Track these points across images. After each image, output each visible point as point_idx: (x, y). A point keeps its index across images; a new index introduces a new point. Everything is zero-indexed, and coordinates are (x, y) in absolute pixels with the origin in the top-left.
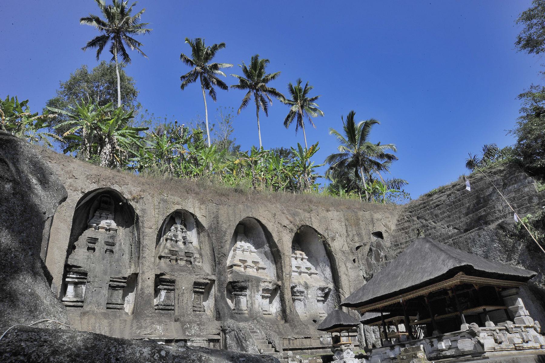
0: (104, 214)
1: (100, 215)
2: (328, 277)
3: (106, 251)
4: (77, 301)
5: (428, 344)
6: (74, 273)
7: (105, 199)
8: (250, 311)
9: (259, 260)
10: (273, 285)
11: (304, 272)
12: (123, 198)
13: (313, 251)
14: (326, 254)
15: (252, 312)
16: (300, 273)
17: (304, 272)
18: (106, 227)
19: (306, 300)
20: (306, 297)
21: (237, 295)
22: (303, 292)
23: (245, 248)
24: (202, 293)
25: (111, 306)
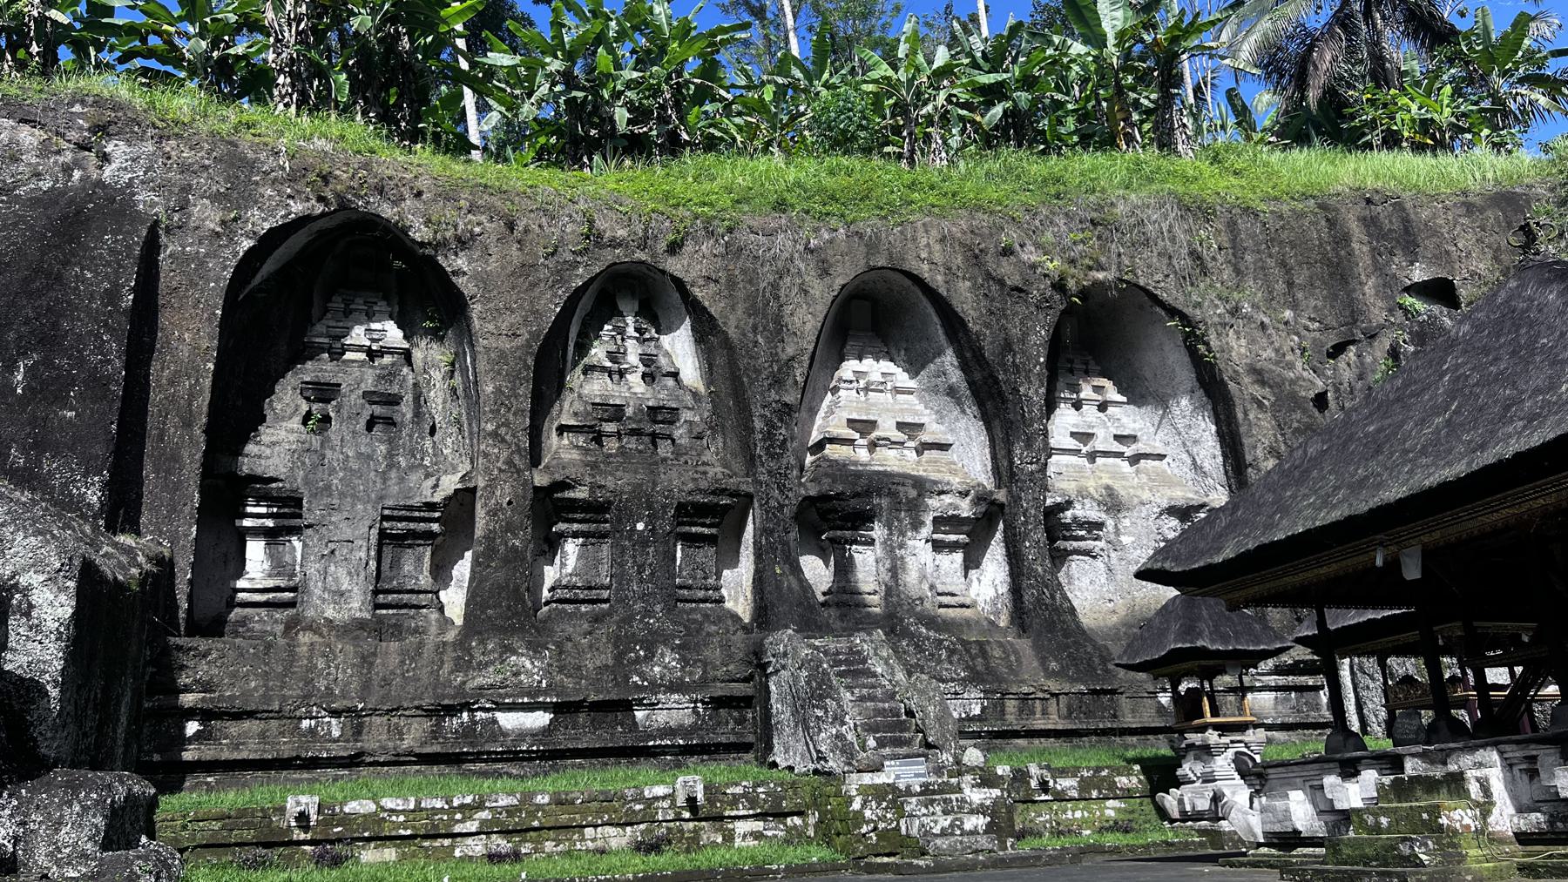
1: (347, 305)
2: (1207, 466)
4: (277, 589)
5: (1516, 769)
8: (889, 592)
9: (926, 417)
11: (1106, 454)
12: (409, 244)
13: (1148, 374)
14: (1198, 380)
15: (895, 599)
16: (1092, 457)
17: (1106, 454)
19: (1113, 555)
20: (1115, 545)
21: (839, 543)
22: (1100, 525)
24: (711, 540)
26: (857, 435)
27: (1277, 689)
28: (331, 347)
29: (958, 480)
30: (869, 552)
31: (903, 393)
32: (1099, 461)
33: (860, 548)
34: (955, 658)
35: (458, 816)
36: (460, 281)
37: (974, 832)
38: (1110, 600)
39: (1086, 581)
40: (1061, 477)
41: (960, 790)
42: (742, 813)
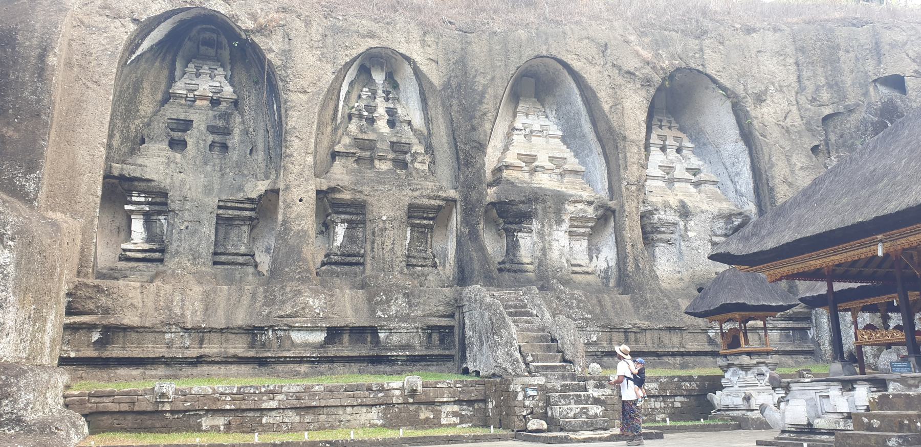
0: (207, 68)
2: (743, 190)
3: (211, 147)
6: (141, 192)
7: (207, 35)
8: (540, 265)
10: (596, 209)
11: (680, 180)
13: (708, 129)
15: (544, 268)
17: (680, 180)
18: (211, 95)
19: (682, 243)
20: (684, 238)
23: (534, 129)
25: (223, 258)
26: (523, 165)
27: (782, 329)
28: (187, 97)
29: (587, 194)
30: (529, 238)
31: (554, 138)
32: (677, 185)
33: (523, 235)
34: (581, 305)
35: (265, 398)
36: (270, 56)
37: (596, 416)
38: (679, 272)
39: (664, 259)
40: (652, 194)
41: (586, 390)
42: (445, 400)
